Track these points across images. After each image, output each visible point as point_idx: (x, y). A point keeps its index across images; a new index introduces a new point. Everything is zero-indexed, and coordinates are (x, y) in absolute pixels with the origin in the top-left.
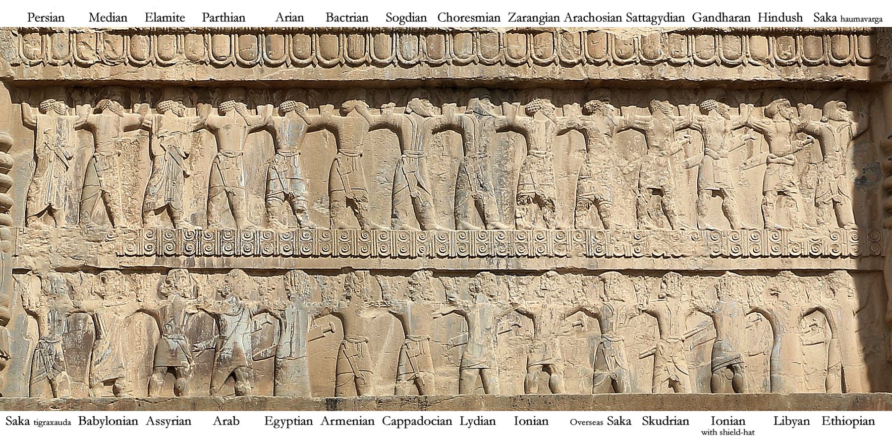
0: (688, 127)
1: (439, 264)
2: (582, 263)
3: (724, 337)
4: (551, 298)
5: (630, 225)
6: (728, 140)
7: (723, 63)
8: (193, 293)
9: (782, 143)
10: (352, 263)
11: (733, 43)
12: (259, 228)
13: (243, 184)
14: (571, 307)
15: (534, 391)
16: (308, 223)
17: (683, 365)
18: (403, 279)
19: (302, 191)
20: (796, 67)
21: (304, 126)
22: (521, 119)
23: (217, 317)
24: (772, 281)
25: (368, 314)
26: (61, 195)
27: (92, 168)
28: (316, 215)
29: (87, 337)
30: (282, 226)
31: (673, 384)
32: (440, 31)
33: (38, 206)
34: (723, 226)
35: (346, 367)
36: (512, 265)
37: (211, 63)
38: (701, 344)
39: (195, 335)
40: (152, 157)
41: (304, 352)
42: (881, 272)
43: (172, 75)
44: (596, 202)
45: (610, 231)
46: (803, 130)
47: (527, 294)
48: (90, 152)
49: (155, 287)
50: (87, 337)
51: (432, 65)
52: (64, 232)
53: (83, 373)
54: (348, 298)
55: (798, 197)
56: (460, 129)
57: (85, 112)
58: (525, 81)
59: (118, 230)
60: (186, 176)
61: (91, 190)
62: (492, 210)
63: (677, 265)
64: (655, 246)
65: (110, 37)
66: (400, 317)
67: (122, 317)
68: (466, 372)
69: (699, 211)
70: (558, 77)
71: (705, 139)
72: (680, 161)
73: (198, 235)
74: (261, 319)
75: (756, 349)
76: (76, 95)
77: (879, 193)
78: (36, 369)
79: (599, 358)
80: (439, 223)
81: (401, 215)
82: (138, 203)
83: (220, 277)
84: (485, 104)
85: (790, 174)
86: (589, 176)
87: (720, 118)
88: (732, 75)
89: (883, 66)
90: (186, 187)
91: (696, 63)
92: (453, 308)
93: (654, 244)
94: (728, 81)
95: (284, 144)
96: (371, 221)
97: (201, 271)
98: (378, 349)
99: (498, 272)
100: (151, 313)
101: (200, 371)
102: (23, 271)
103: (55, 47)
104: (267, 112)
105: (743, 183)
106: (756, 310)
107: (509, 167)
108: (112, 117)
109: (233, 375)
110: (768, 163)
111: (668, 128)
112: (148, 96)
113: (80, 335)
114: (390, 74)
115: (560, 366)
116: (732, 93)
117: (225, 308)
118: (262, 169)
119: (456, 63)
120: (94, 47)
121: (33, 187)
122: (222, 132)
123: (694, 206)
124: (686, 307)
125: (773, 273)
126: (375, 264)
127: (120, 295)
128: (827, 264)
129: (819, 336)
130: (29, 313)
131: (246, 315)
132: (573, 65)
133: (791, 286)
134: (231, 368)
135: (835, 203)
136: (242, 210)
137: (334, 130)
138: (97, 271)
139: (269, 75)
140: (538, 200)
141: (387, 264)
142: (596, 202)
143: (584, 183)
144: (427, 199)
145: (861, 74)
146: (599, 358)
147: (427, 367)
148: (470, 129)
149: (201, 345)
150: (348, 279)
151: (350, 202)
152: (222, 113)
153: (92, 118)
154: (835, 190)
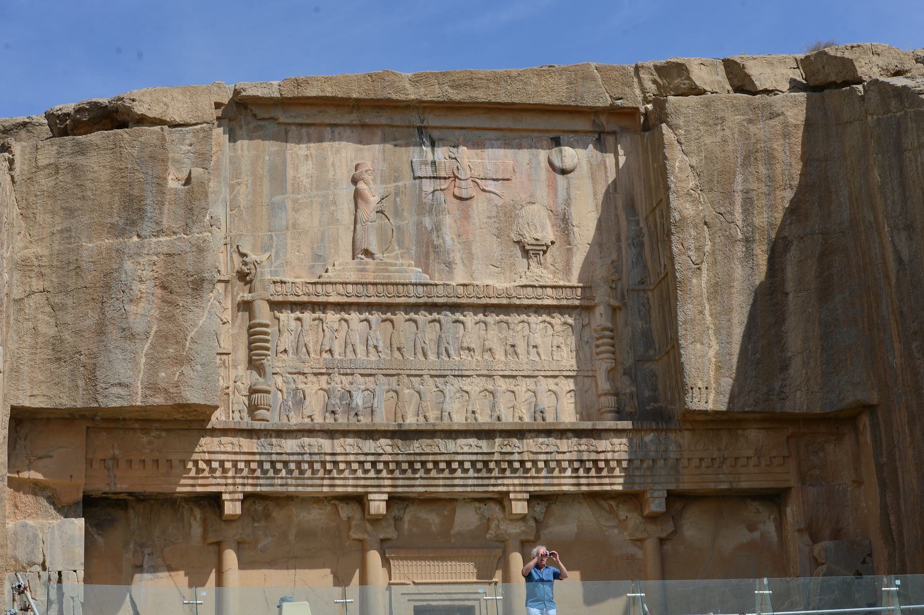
1: (433, 373)
2: (486, 372)
4: (474, 386)
5: (503, 358)
8: (340, 383)
9: (558, 328)
10: (400, 372)
11: (540, 291)
15: (469, 421)
16: (383, 356)
17: (524, 411)
18: (418, 379)
22: (461, 318)
23: (349, 392)
24: (556, 380)
25: (406, 391)
28: (386, 354)
29: (301, 399)
30: (373, 357)
31: (521, 418)
33: (281, 349)
34: (537, 359)
35: (398, 411)
36: (460, 373)
38: (530, 403)
39: (341, 399)
40: (323, 331)
41: (383, 405)
43: (331, 299)
44: (490, 350)
47: (465, 384)
48: (300, 329)
50: (301, 399)
55: (564, 348)
56: (439, 322)
61: (301, 343)
62: (452, 352)
66: (419, 393)
69: (528, 353)
72: (520, 335)
73: (342, 361)
74: (366, 393)
76: (294, 307)
77: (593, 347)
79: (493, 408)
80: (432, 357)
83: (350, 377)
85: (561, 340)
88: (539, 302)
95: (373, 326)
96: (407, 356)
97: (343, 374)
99: (454, 376)
100: (325, 390)
101: (343, 412)
103: (287, 288)
104: (366, 315)
105: (544, 342)
106: (550, 390)
108: (307, 316)
109: (356, 414)
113: (298, 398)
114: (413, 300)
115: (479, 411)
116: (538, 309)
124: (524, 389)
125: (556, 377)
126: (408, 372)
127: (313, 383)
136: (358, 351)
139: (367, 300)
140: (469, 349)
141: (413, 372)
142: (490, 350)
144: (427, 347)
146: (493, 408)
148: (443, 321)
149: (344, 402)
151: (399, 349)
153: (300, 315)
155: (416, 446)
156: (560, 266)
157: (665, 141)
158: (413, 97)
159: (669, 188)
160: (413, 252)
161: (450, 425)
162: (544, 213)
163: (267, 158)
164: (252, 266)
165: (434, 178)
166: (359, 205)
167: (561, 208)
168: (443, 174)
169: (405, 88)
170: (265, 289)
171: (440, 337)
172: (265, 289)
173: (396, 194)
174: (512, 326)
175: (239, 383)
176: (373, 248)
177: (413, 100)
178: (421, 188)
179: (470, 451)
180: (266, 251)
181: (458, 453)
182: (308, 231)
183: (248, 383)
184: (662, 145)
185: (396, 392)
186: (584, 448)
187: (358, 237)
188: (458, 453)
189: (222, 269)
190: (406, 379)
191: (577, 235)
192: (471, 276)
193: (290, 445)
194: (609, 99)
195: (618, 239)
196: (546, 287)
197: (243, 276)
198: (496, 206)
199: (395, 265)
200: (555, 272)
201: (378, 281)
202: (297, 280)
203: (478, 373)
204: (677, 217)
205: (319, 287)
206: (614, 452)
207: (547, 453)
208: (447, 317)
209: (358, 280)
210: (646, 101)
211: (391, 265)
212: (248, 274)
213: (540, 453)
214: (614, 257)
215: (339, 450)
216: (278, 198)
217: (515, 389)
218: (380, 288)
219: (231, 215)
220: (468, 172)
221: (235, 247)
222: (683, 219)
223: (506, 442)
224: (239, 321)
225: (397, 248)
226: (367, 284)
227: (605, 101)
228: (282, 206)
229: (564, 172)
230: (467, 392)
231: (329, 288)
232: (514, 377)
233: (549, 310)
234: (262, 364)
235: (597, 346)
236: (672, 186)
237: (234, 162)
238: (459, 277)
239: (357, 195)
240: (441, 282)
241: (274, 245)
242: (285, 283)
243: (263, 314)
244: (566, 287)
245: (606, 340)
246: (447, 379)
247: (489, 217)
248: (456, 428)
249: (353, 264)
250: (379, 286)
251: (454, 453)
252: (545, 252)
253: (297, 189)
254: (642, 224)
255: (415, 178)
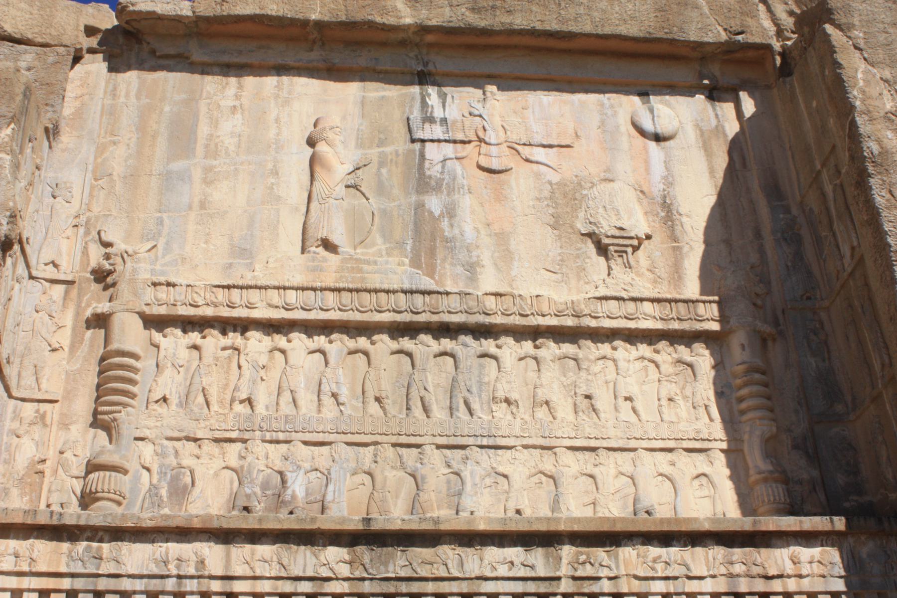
0: (604, 357)
3: (640, 491)
4: (519, 466)
5: (571, 417)
6: (631, 366)
7: (626, 318)
10: (378, 438)
11: (631, 306)
12: (313, 414)
13: (302, 385)
14: (533, 471)
16: (347, 411)
18: (415, 451)
19: (344, 394)
20: (672, 321)
21: (346, 351)
22: (493, 350)
23: (281, 473)
24: (669, 456)
26: (174, 390)
27: (197, 373)
30: (330, 410)
32: (438, 293)
33: (158, 396)
34: (633, 418)
36: (491, 442)
37: (283, 307)
39: (265, 486)
40: (240, 367)
42: (742, 451)
43: (256, 314)
45: (557, 421)
46: (680, 361)
47: (502, 461)
48: (196, 363)
49: (237, 453)
50: (185, 487)
51: (433, 313)
52: (173, 413)
53: (180, 510)
54: (376, 462)
57: (195, 337)
58: (496, 325)
59: (212, 413)
60: (262, 380)
61: (197, 387)
62: (476, 406)
63: (605, 444)
64: (589, 430)
65: (214, 289)
67: (212, 472)
68: (461, 513)
69: (616, 409)
70: (517, 323)
71: (616, 365)
73: (269, 418)
75: (663, 501)
76: (189, 327)
77: (734, 401)
78: (146, 505)
79: (555, 504)
80: (439, 413)
81: (413, 407)
82: (228, 397)
83: (284, 447)
84: (468, 339)
86: (542, 386)
87: (624, 352)
88: (632, 325)
89: (728, 322)
90: (262, 387)
91: (608, 317)
92: (451, 470)
93: (588, 430)
94: (629, 329)
95: (332, 360)
97: (271, 442)
98: (397, 497)
99: (481, 447)
101: (267, 509)
102: (142, 439)
104: (320, 341)
106: (661, 475)
107: (486, 379)
108: (213, 341)
110: (659, 381)
111: (592, 357)
112: (239, 329)
116: (633, 337)
117: (287, 467)
118: (317, 378)
119: (449, 312)
120: (202, 295)
121: (154, 384)
122: (289, 353)
123: (613, 406)
124: (613, 472)
125: (670, 450)
127: (211, 457)
128: (705, 445)
129: (706, 492)
130: (144, 467)
131: (302, 472)
132: (527, 316)
133: (683, 459)
134: (290, 509)
135: (706, 406)
136: (301, 402)
137: (366, 354)
138: (196, 440)
140: (507, 401)
141: (404, 440)
142: (547, 403)
143: (538, 391)
144: (431, 399)
145: (715, 326)
146: (555, 504)
147: (433, 510)
150: (376, 450)
151: (378, 399)
152: (289, 341)
154: (705, 398)
155: (399, 562)
156: (663, 271)
157: (835, 43)
158: (408, 21)
159: (852, 108)
160: (408, 248)
161: (468, 522)
162: (630, 195)
163: (167, 109)
164: (119, 260)
165: (446, 141)
166: (316, 175)
167: (657, 188)
168: (460, 136)
169: (395, 9)
170: (135, 294)
171: (454, 380)
172: (135, 294)
173: (381, 164)
174: (584, 365)
175: (68, 455)
176: (335, 239)
177: (409, 26)
178: (422, 156)
179: (511, 574)
180: (148, 240)
181: (487, 579)
182: (226, 212)
183: (85, 454)
184: (832, 50)
185: (369, 474)
186: (738, 569)
187: (312, 220)
188: (487, 579)
189: (64, 264)
190: (390, 452)
191: (687, 227)
192: (511, 286)
193: (137, 557)
194: (723, 33)
195: (758, 234)
196: (642, 300)
197: (101, 276)
198: (550, 183)
199: (375, 263)
200: (655, 282)
201: (341, 285)
202: (197, 283)
203: (526, 442)
204: (875, 148)
205: (236, 292)
206: (800, 576)
207: (667, 578)
208: (467, 347)
209: (305, 285)
210: (780, 33)
211: (368, 262)
212: (110, 273)
213: (653, 578)
214: (754, 258)
215: (239, 571)
216: (177, 165)
217: (596, 471)
218: (346, 297)
219: (92, 188)
220: (502, 133)
221: (94, 234)
222: (884, 152)
223: (583, 558)
224: (85, 347)
225: (379, 240)
226: (322, 289)
227: (717, 34)
228: (184, 177)
229: (658, 138)
230: (506, 476)
231: (254, 296)
232: (593, 449)
233: (650, 337)
234: (115, 420)
235: (741, 400)
236: (858, 103)
237: (111, 113)
238: (489, 281)
239: (313, 161)
240: (456, 291)
241: (165, 231)
242: (174, 285)
243: (130, 333)
244: (676, 301)
245: (755, 388)
246: (467, 452)
247: (538, 199)
248: (482, 526)
249: (300, 259)
250: (345, 294)
251: (478, 578)
252: (636, 249)
253: (212, 151)
254: (795, 211)
255: (413, 141)
